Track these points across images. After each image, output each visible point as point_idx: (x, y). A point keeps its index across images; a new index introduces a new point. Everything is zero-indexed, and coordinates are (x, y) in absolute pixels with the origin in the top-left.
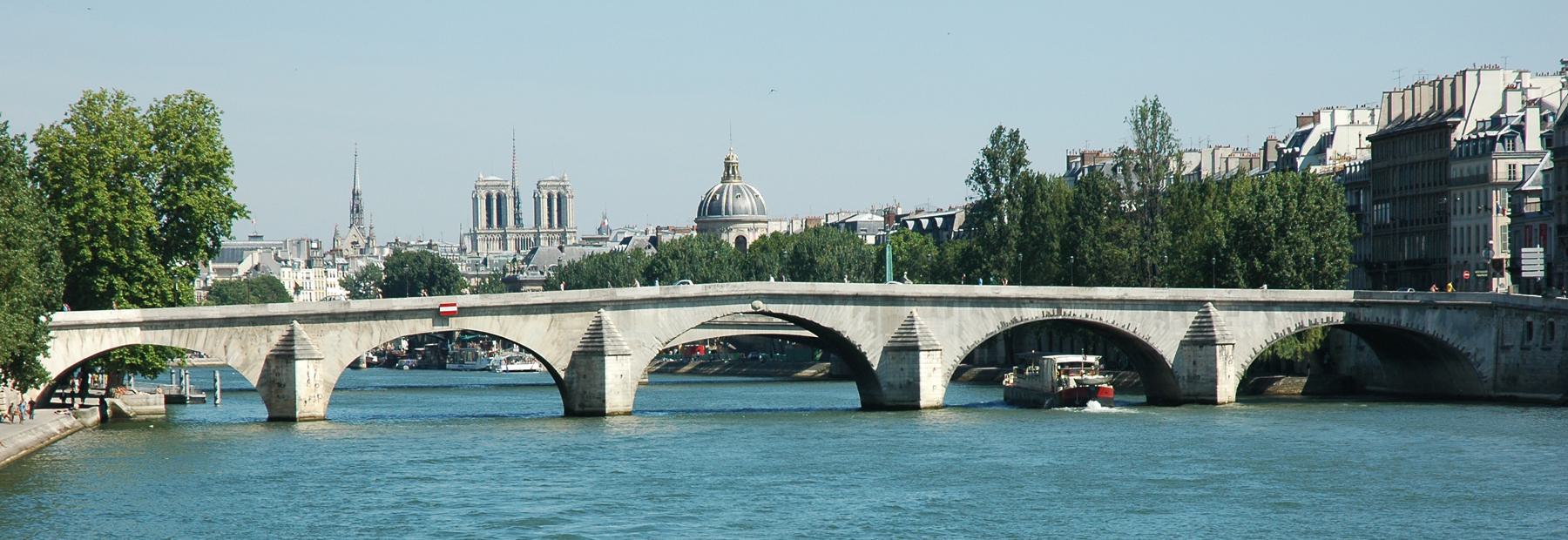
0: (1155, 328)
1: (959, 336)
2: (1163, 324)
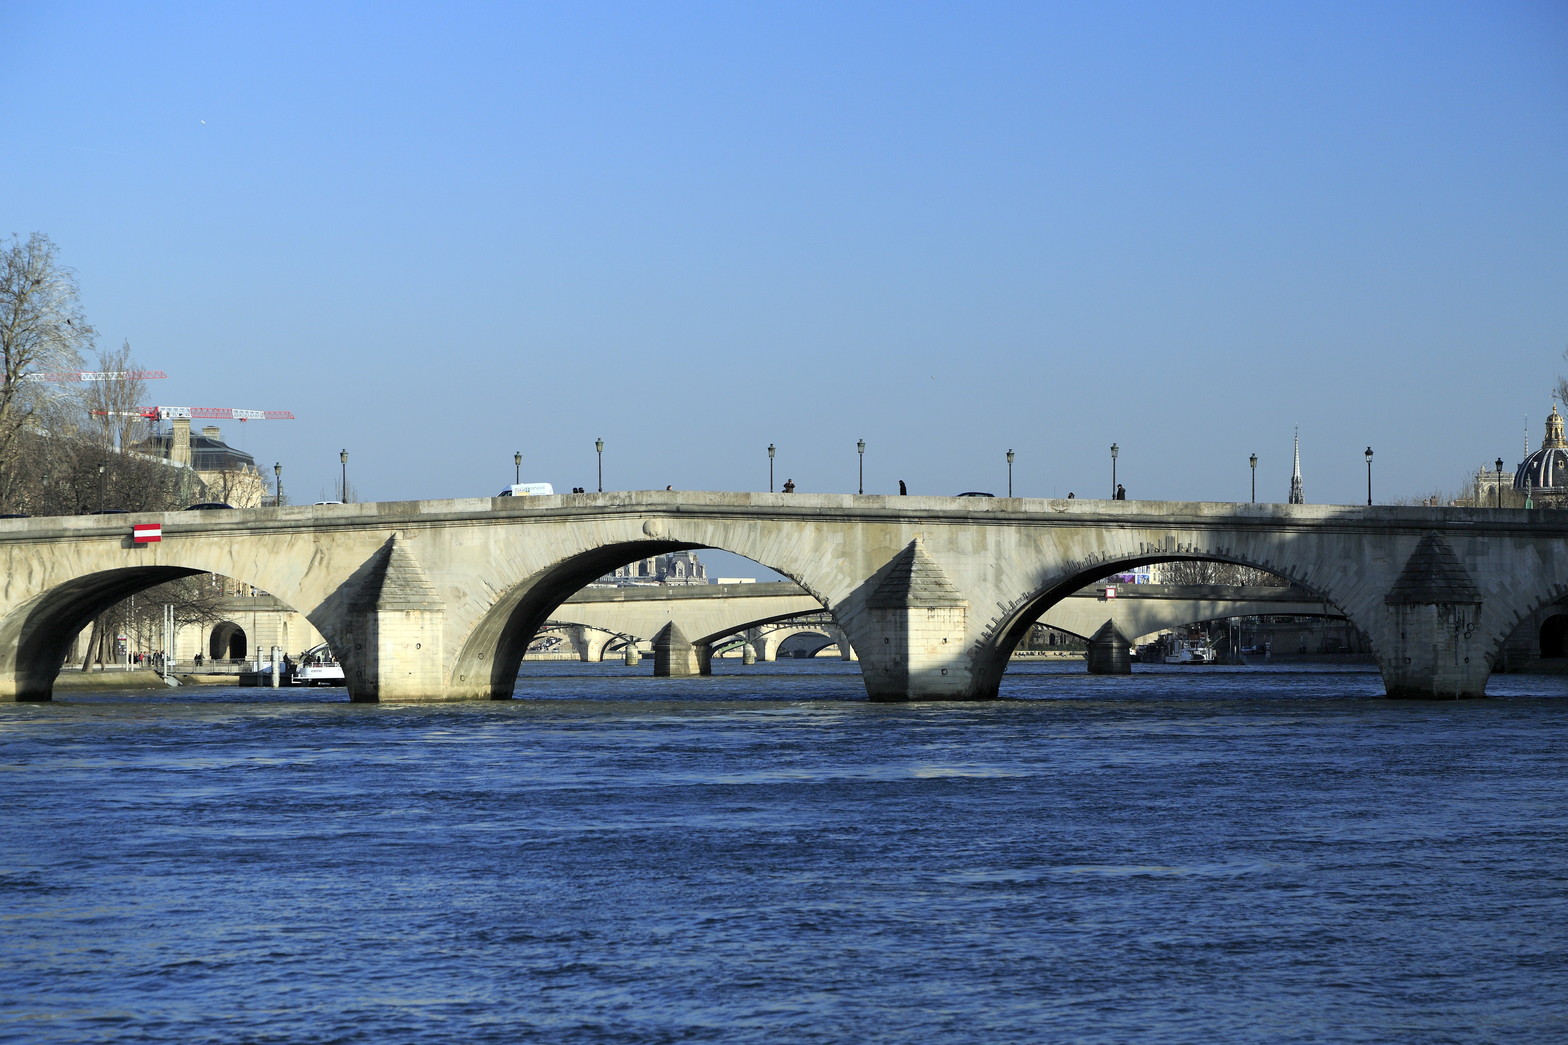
0: (1339, 574)
1: (997, 586)
2: (1354, 567)
